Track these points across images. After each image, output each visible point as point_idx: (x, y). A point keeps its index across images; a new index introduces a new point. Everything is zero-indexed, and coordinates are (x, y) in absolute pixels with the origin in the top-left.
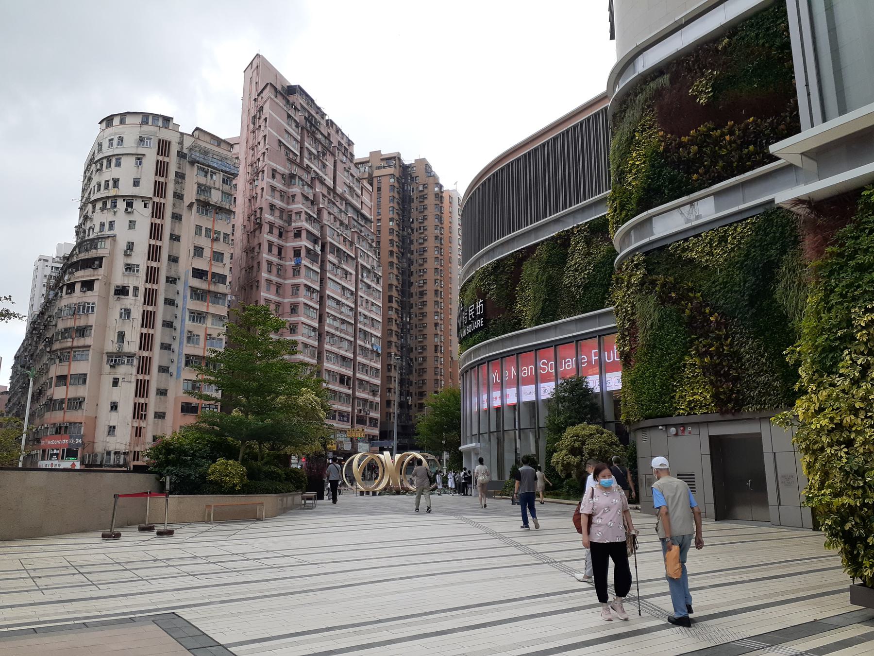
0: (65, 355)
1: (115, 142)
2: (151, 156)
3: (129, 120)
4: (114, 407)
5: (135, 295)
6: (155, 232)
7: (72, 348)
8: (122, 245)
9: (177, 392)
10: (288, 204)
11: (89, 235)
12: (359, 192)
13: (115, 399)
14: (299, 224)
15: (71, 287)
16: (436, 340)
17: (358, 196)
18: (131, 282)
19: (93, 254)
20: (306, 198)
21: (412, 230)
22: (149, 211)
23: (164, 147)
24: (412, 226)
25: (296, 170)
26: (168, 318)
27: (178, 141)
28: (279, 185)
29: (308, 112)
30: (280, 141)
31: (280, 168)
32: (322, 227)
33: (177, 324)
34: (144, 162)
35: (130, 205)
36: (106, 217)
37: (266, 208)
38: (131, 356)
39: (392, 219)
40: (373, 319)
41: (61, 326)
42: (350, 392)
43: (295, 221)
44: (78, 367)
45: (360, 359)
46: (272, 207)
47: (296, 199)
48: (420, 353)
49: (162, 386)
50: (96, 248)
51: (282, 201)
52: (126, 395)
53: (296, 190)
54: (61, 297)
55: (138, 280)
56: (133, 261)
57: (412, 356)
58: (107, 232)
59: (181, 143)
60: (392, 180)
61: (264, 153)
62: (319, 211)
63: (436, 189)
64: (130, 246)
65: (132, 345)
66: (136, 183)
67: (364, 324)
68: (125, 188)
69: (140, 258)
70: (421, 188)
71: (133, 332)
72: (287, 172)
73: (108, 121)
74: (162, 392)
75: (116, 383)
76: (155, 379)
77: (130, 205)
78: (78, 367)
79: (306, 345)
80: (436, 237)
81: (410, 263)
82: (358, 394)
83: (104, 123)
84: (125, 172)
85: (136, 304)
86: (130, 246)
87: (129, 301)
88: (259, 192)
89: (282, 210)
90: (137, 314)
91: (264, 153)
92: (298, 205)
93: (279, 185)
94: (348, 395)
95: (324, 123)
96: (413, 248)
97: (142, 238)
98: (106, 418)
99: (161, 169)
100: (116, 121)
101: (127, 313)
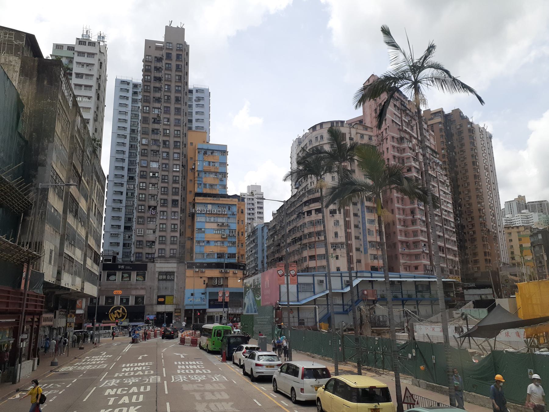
0: (312, 246)
1: (319, 138)
3: (324, 126)
5: (340, 213)
7: (315, 242)
9: (367, 260)
10: (401, 154)
11: (311, 185)
12: (429, 137)
13: (338, 266)
14: (409, 164)
15: (309, 213)
16: (481, 219)
17: (428, 140)
20: (410, 148)
21: (455, 153)
24: (455, 150)
25: (403, 134)
26: (356, 223)
27: (348, 132)
28: (396, 145)
29: (401, 100)
30: (393, 121)
31: (396, 136)
32: (419, 163)
33: (360, 226)
37: (391, 157)
38: (342, 244)
39: (443, 149)
40: (449, 212)
41: (306, 231)
42: (444, 255)
43: (407, 163)
45: (446, 236)
46: (394, 157)
47: (406, 151)
48: (470, 229)
49: (359, 258)
51: (398, 152)
52: (342, 263)
53: (405, 145)
54: (304, 217)
57: (465, 231)
59: (350, 133)
60: (440, 125)
61: (386, 129)
62: (417, 154)
63: (469, 126)
65: (342, 238)
67: (446, 215)
70: (458, 127)
72: (399, 136)
73: (314, 128)
74: (359, 261)
75: (337, 258)
76: (355, 255)
79: (422, 231)
80: (472, 156)
81: (457, 173)
82: (448, 257)
83: (311, 129)
88: (385, 150)
89: (399, 158)
90: (342, 223)
91: (386, 129)
92: (409, 154)
93: (396, 145)
94: (443, 257)
95: (407, 102)
96: (457, 164)
100: (318, 128)
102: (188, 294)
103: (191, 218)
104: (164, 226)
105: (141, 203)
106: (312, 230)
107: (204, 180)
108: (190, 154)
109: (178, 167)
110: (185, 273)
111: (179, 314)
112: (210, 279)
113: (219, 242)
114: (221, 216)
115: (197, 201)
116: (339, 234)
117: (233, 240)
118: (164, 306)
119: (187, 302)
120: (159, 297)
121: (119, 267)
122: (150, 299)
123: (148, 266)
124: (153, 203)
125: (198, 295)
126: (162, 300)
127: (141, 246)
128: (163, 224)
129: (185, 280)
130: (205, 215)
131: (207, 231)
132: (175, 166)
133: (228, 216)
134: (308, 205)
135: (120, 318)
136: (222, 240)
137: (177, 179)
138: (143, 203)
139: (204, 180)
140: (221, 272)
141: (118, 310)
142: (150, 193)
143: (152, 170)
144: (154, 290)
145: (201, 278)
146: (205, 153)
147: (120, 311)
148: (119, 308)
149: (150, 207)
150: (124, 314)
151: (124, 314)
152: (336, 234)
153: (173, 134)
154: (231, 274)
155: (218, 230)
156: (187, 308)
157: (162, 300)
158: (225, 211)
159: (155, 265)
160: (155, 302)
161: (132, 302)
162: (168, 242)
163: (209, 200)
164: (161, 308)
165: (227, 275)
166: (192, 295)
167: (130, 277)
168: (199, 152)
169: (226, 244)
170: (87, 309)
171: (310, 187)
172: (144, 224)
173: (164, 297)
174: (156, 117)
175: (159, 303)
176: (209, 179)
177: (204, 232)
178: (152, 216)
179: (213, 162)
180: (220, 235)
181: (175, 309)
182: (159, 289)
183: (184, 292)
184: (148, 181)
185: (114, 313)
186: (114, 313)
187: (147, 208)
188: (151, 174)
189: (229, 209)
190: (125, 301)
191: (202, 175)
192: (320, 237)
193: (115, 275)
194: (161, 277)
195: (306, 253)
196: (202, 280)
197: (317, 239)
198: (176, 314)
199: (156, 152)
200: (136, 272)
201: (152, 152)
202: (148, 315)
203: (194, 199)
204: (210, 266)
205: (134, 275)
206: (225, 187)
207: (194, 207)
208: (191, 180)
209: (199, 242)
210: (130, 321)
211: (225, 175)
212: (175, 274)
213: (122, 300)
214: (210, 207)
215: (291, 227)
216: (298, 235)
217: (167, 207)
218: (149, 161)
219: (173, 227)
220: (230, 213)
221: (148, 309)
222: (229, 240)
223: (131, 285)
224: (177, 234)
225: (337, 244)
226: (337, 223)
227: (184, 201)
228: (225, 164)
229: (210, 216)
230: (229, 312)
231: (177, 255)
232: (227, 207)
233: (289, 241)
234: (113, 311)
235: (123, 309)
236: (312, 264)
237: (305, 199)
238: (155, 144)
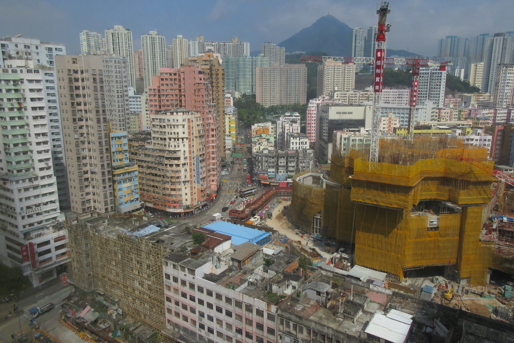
0: (173, 183)
2: (186, 123)
4: (186, 194)
6: (190, 147)
8: (182, 151)
15: (171, 165)
18: (186, 162)
19: (175, 155)
38: (188, 181)
44: (178, 187)
55: (188, 161)
56: (186, 156)
64: (184, 152)
66: (184, 133)
68: (181, 135)
69: (187, 155)
78: (178, 187)
84: (180, 130)
86: (184, 152)
90: (188, 170)
97: (187, 148)
98: (184, 197)
101: (186, 170)
131: (123, 189)
152: (185, 177)
177: (122, 190)
191: (115, 153)
226: (186, 170)
236: (173, 193)
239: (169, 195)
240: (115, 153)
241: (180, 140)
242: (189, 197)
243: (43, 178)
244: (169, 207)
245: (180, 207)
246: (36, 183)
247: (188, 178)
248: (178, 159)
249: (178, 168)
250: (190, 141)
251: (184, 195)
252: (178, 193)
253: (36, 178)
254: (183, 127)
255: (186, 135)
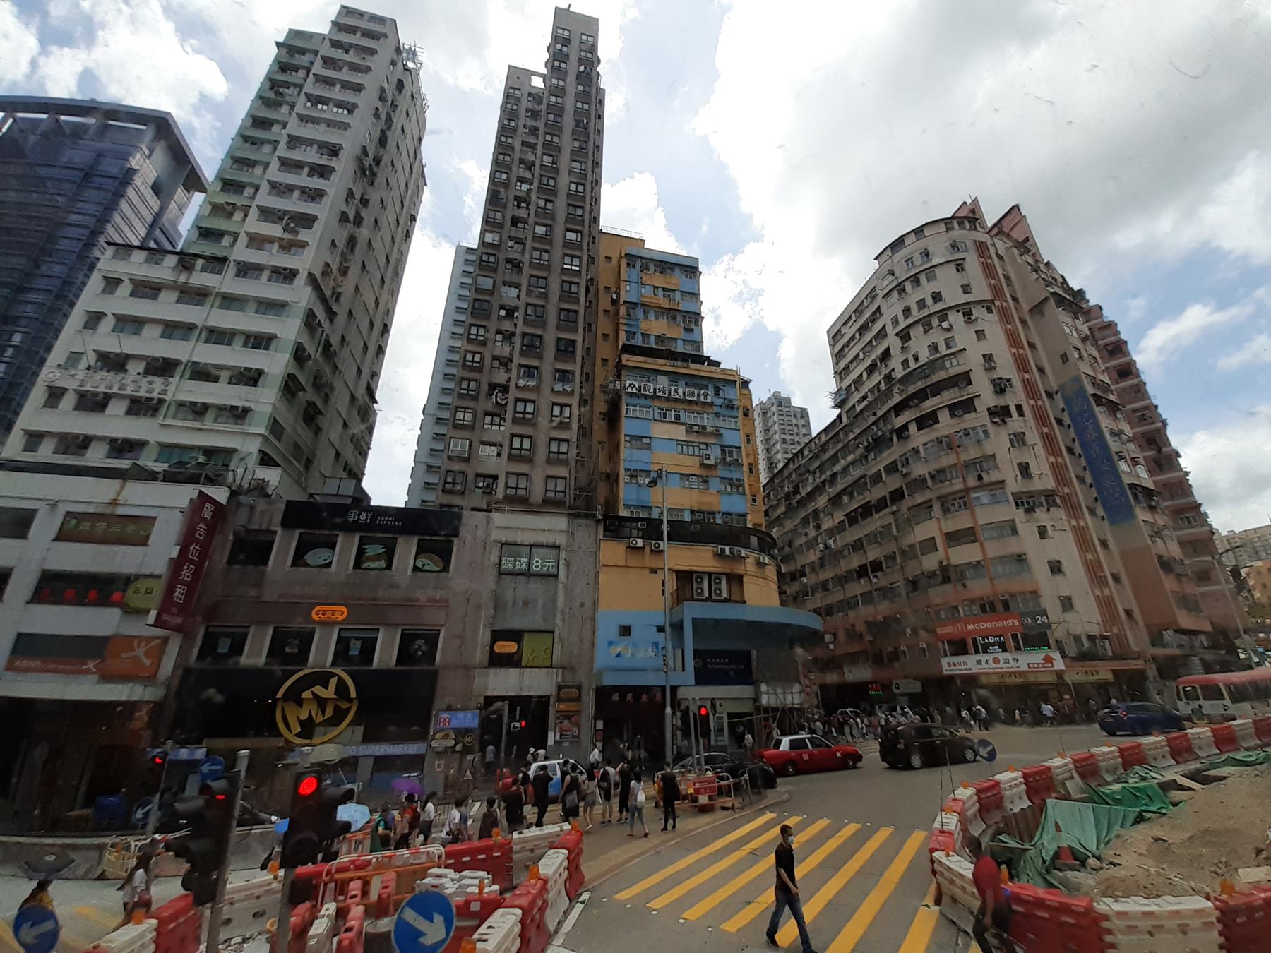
3: (927, 232)
4: (1056, 568)
5: (1021, 414)
6: (1013, 340)
7: (968, 490)
18: (1010, 400)
22: (994, 317)
23: (981, 248)
34: (967, 265)
35: (967, 314)
36: (937, 337)
38: (1049, 498)
50: (944, 368)
58: (944, 351)
64: (988, 358)
66: (966, 289)
68: (954, 296)
69: (1006, 368)
71: (1040, 463)
77: (967, 314)
85: (1025, 425)
86: (988, 358)
87: (1015, 424)
90: (1033, 437)
97: (997, 343)
98: (1050, 590)
99: (989, 270)
102: (607, 629)
103: (603, 424)
104: (530, 408)
105: (470, 375)
106: (947, 460)
107: (643, 325)
108: (605, 279)
109: (576, 261)
110: (596, 554)
111: (573, 707)
112: (685, 577)
113: (693, 479)
114: (695, 408)
115: (624, 362)
116: (1034, 469)
117: (735, 475)
118: (514, 671)
119: (603, 657)
120: (497, 636)
121: (352, 517)
122: (461, 641)
123: (464, 520)
124: (501, 377)
125: (644, 633)
126: (511, 647)
127: (458, 487)
128: (525, 401)
129: (597, 575)
130: (648, 402)
131: (654, 444)
132: (567, 260)
133: (716, 409)
134: (917, 405)
135: (320, 724)
136: (704, 473)
137: (574, 288)
138: (477, 376)
139: (643, 325)
140: (720, 556)
141: (318, 690)
142: (496, 354)
143: (505, 301)
144: (478, 607)
145: (654, 571)
146: (644, 268)
147: (329, 693)
148: (322, 678)
149: (492, 387)
150: (344, 706)
151: (344, 706)
152: (1024, 469)
153: (568, 80)
154: (750, 565)
155: (688, 444)
156: (608, 680)
157: (511, 647)
158: (706, 395)
159: (489, 521)
160: (480, 655)
161: (385, 654)
162: (541, 456)
163: (660, 364)
164: (504, 682)
165: (739, 569)
166: (626, 631)
167: (389, 556)
168: (628, 265)
169: (715, 485)
170: (176, 682)
171: (899, 374)
172: (472, 428)
173: (516, 635)
174: (523, 195)
175: (498, 661)
176: (657, 326)
177: (648, 447)
178: (497, 410)
179: (664, 289)
180: (696, 461)
181: (560, 687)
182: (498, 603)
183: (593, 619)
184: (493, 325)
185: (300, 703)
186: (300, 703)
187: (485, 388)
188: (503, 313)
189: (717, 394)
190: (352, 652)
192: (984, 475)
193: (333, 547)
194: (508, 564)
195: (928, 529)
196: (658, 578)
197: (972, 482)
198: (562, 706)
199: (517, 265)
200: (414, 541)
201: (509, 266)
202: (449, 708)
203: (620, 360)
204: (682, 533)
205: (406, 550)
206: (699, 344)
207: (619, 376)
208: (605, 336)
209: (633, 474)
210: (367, 739)
211: (697, 317)
212: (563, 555)
213: (343, 643)
214: (663, 381)
215: (840, 487)
216: (875, 494)
217: (540, 357)
218: (499, 282)
219: (556, 411)
220: (718, 401)
221: (449, 685)
222: (722, 472)
223: (392, 586)
224: (572, 435)
225: (1031, 495)
226: (1018, 440)
227: (587, 380)
228: (695, 295)
229: (665, 405)
230: (764, 700)
231: (569, 499)
232: (711, 387)
233: (827, 524)
234: (294, 696)
235: (340, 679)
236: (963, 555)
237: (897, 399)
238: (518, 247)
239: (946, 574)
240: (641, 315)
241: (956, 318)
242: (1075, 578)
243: (245, 270)
244: (959, 647)
245: (1036, 639)
246: (200, 279)
247: (1044, 480)
248: (965, 378)
249: (970, 420)
250: (1005, 316)
251: (1040, 571)
252: (995, 549)
253: (217, 263)
254: (960, 267)
255: (981, 291)
